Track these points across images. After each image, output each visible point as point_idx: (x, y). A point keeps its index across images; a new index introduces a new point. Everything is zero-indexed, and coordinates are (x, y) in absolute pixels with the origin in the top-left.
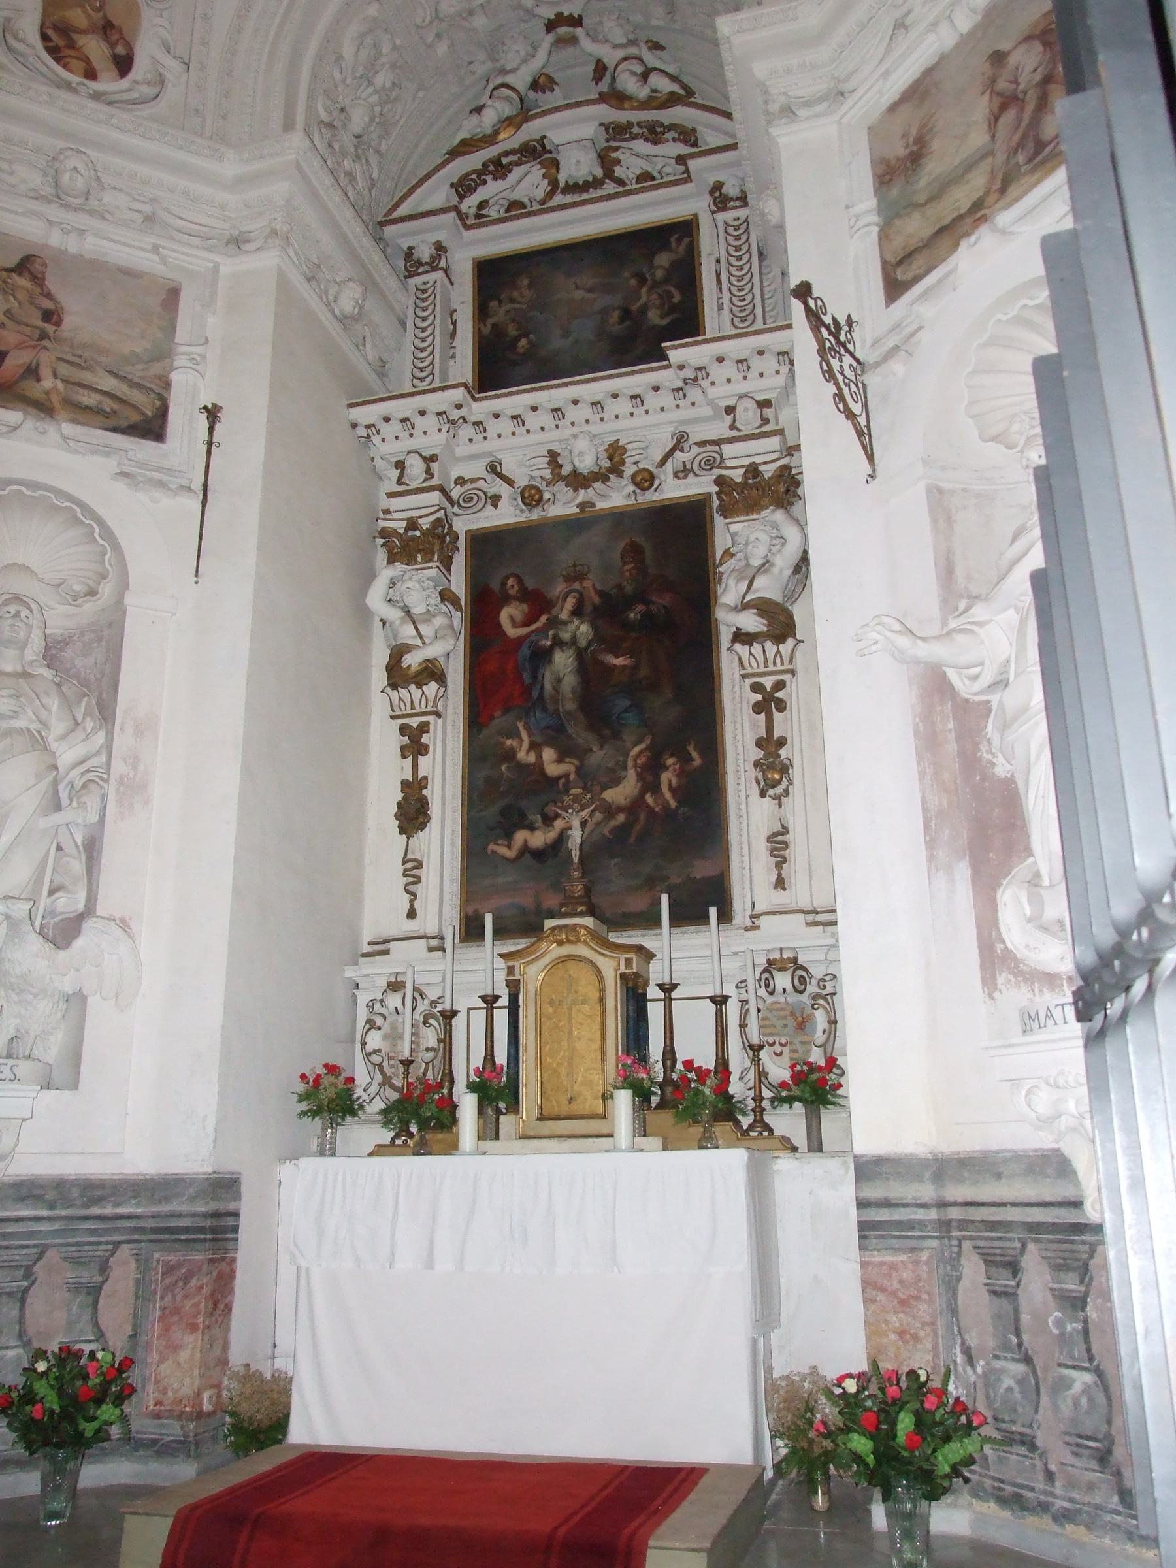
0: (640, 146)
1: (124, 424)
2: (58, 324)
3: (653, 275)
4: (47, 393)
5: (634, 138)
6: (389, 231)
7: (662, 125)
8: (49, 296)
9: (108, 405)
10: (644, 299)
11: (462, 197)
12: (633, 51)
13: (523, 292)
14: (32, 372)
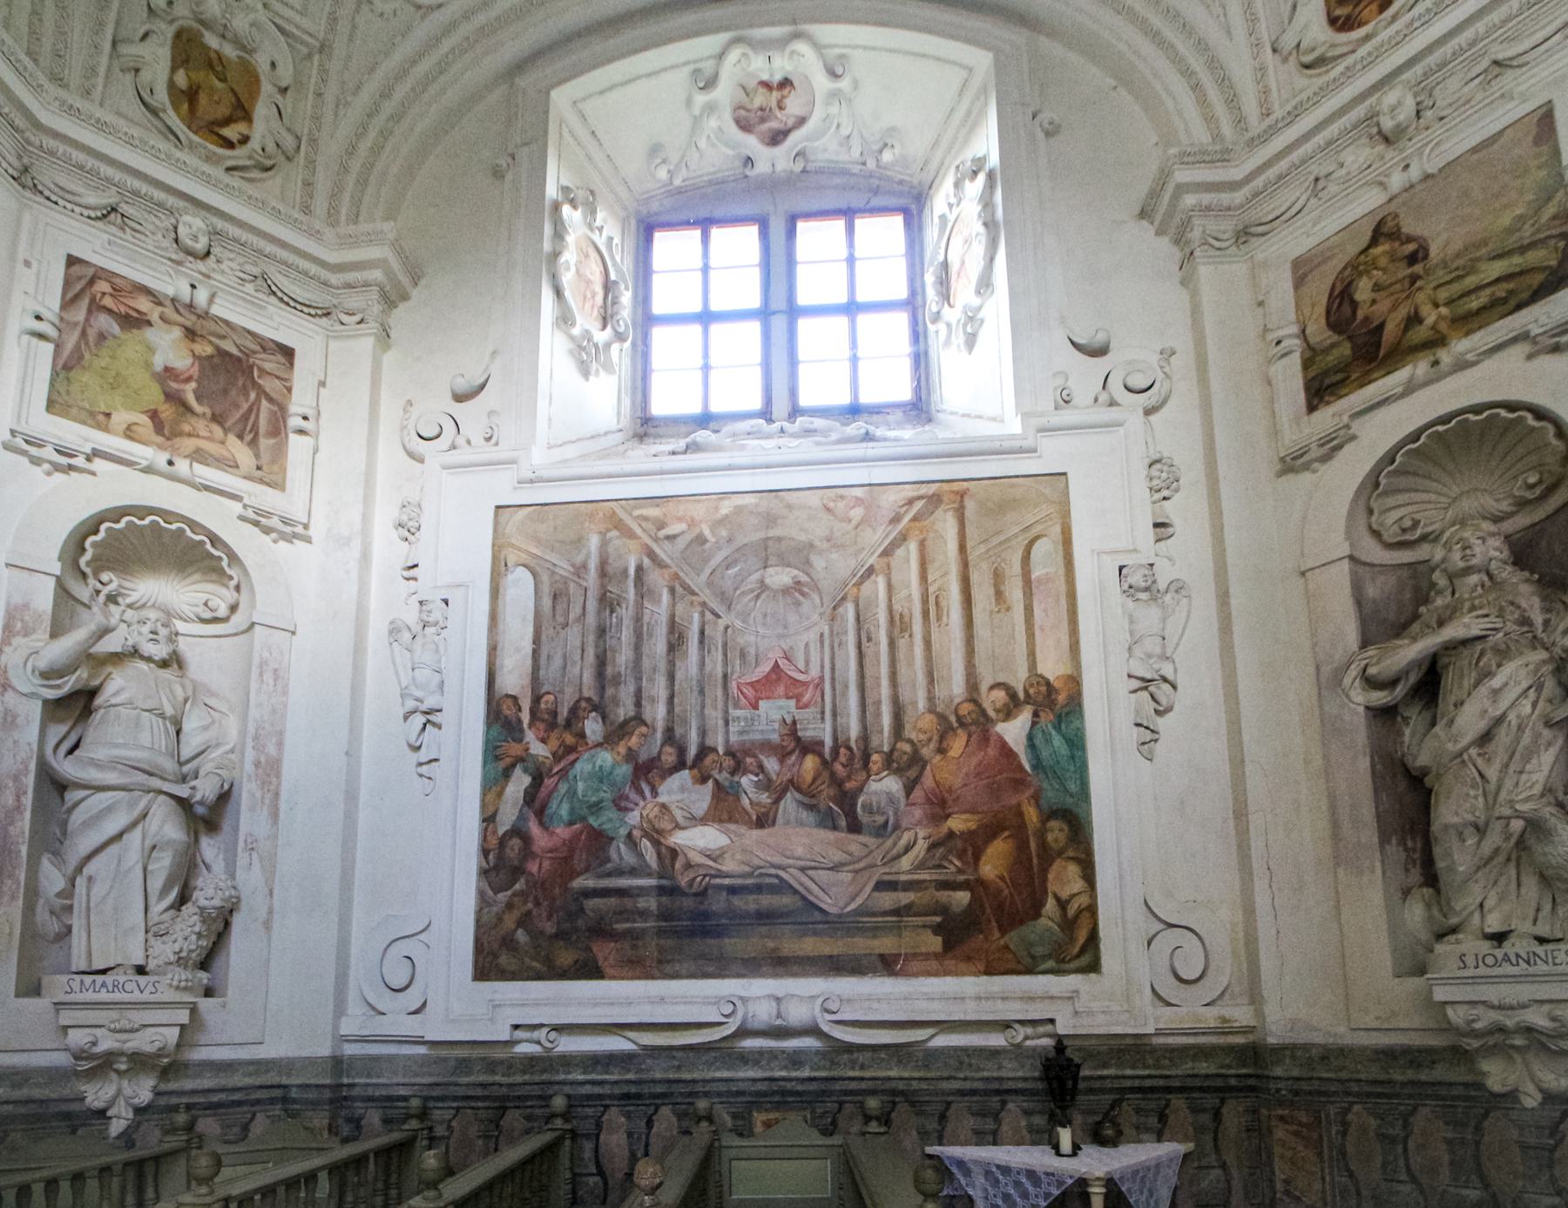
1: (1525, 295)
2: (1426, 257)
4: (1433, 328)
8: (1410, 239)
9: (1500, 291)
14: (1414, 319)
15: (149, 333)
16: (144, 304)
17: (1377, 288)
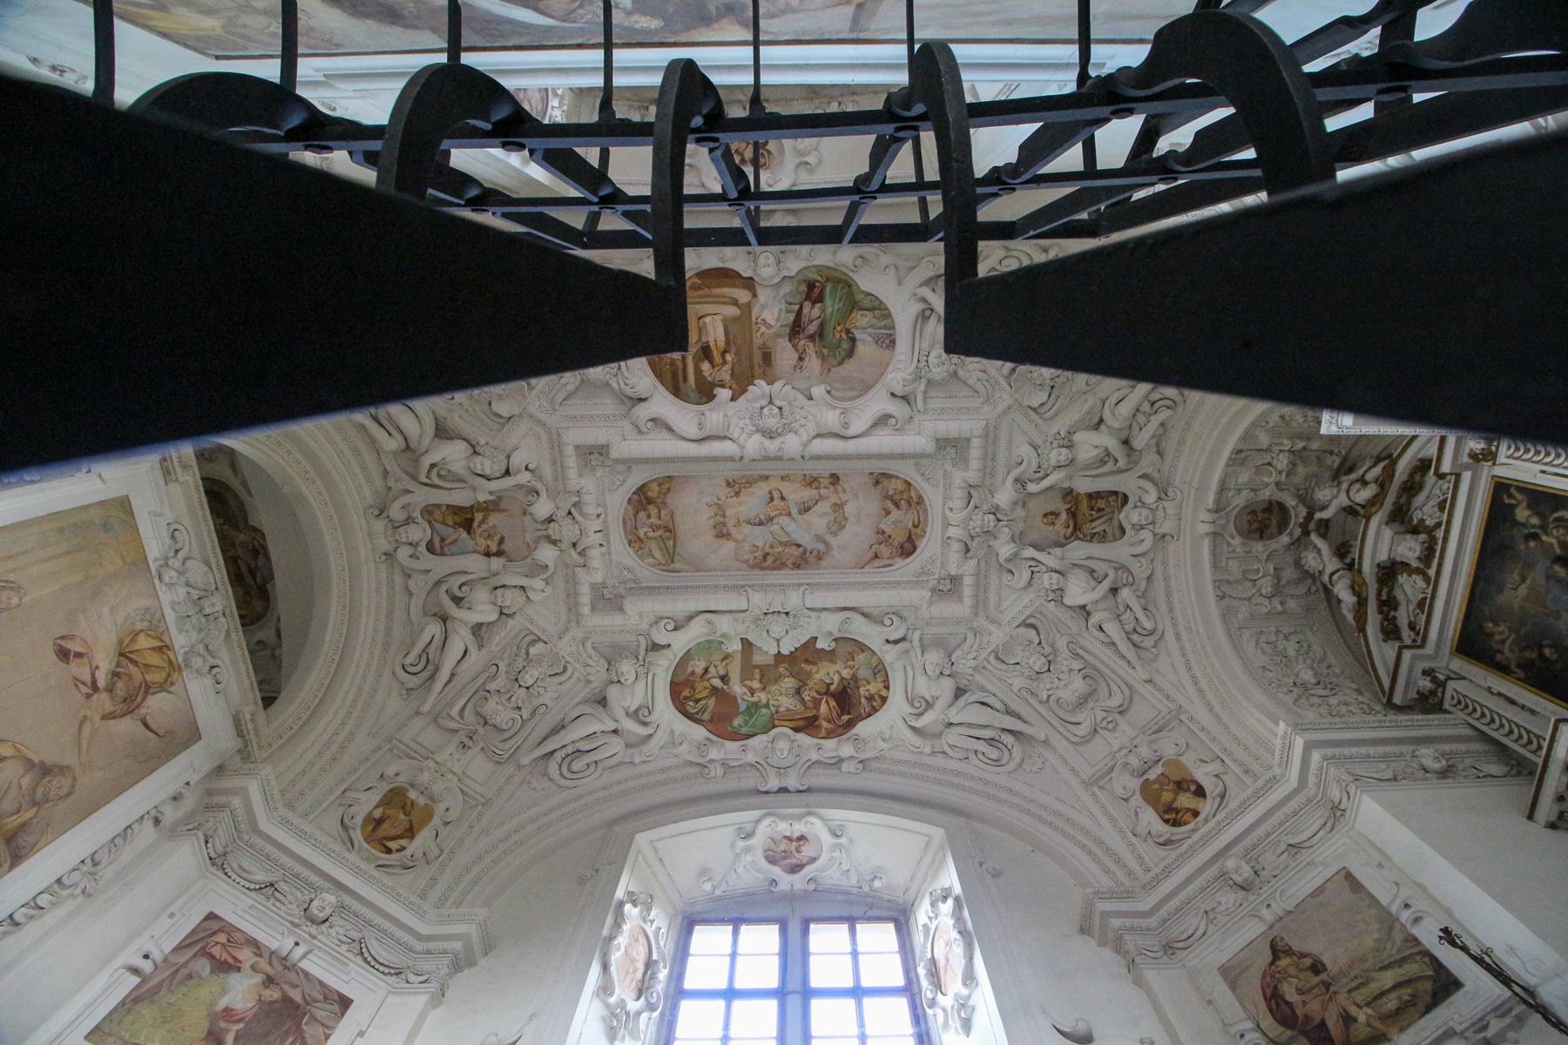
0: (1420, 498)
3: (1533, 526)
5: (1409, 504)
6: (1398, 699)
7: (1405, 482)
10: (1553, 541)
11: (1399, 638)
12: (1344, 486)
13: (1500, 632)
15: (233, 979)
16: (245, 955)
17: (1300, 992)
